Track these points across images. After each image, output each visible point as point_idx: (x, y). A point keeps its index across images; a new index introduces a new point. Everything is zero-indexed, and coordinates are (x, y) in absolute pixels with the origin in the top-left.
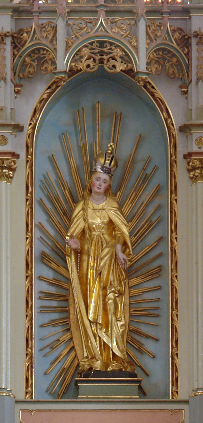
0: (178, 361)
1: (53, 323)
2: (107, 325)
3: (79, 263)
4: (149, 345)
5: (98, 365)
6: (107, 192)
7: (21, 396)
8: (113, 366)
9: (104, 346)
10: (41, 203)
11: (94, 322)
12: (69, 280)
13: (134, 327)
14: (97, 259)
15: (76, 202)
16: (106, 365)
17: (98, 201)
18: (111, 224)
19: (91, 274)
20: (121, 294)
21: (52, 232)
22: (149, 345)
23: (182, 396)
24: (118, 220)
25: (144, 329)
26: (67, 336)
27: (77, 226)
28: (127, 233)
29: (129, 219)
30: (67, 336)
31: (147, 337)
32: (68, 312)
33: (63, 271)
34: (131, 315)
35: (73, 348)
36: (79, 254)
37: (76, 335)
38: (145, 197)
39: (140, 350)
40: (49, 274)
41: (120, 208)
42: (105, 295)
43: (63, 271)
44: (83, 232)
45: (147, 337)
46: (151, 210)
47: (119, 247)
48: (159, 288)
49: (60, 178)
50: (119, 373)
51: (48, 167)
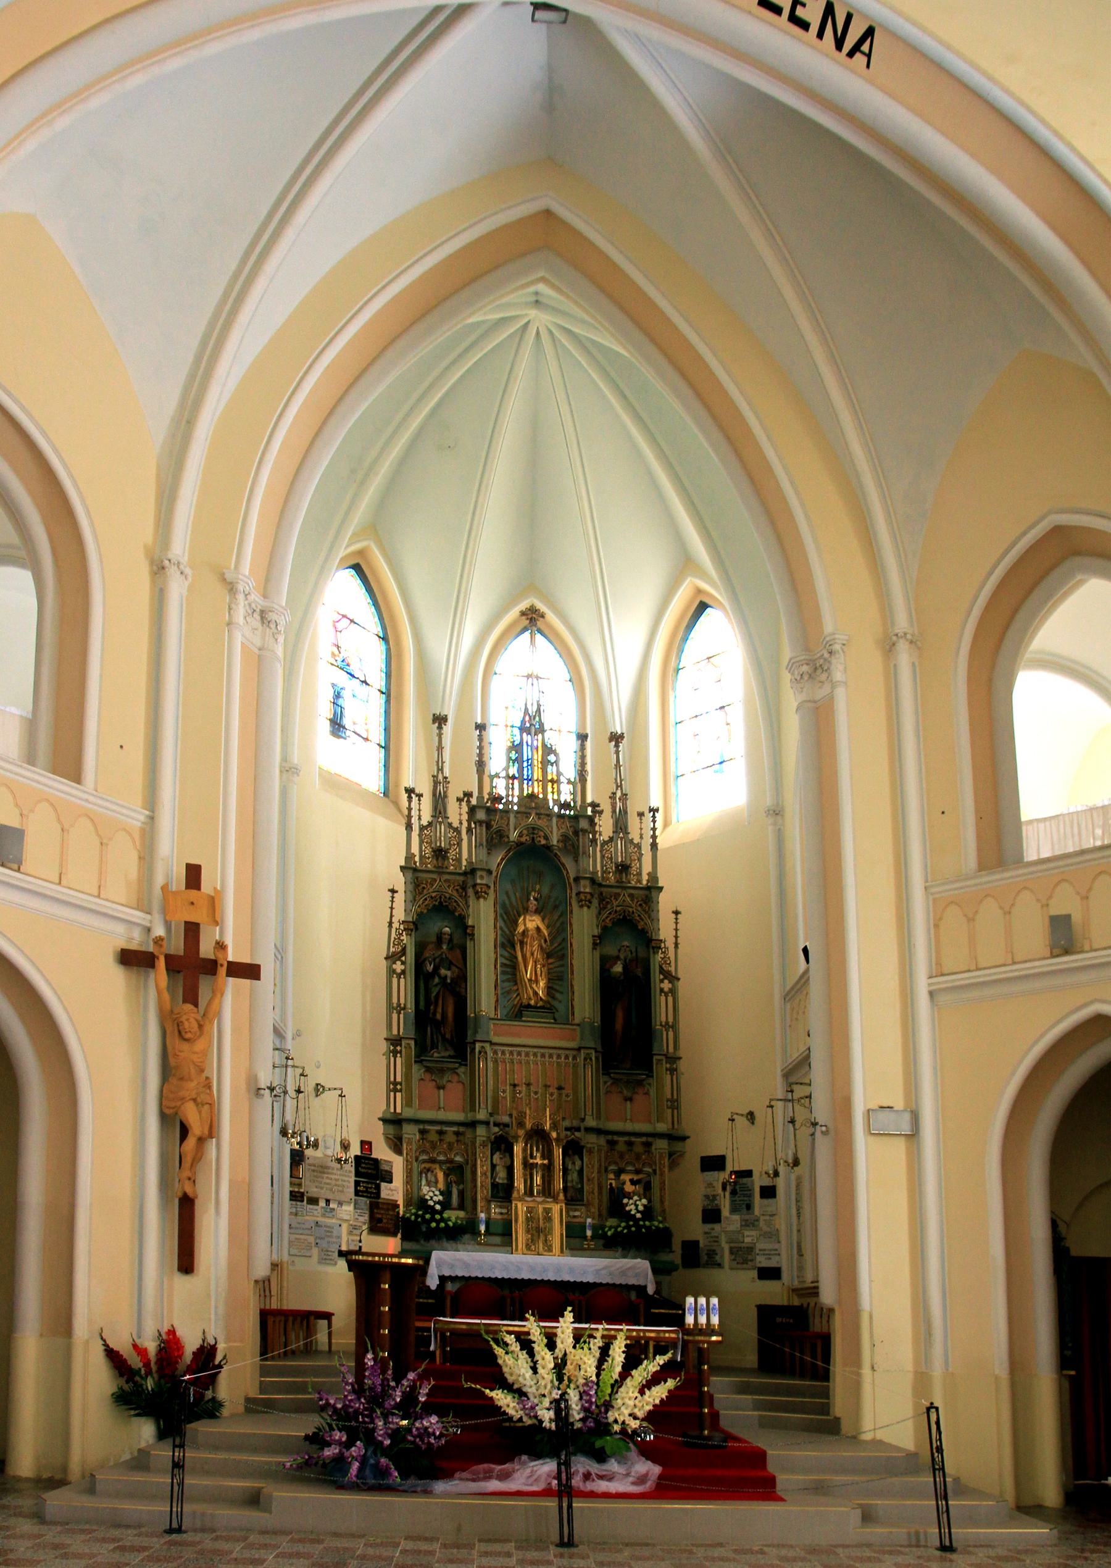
0: (574, 1003)
1: (508, 980)
2: (537, 982)
3: (522, 949)
4: (558, 995)
5: (532, 1002)
6: (537, 911)
7: (492, 1015)
8: (540, 1004)
9: (536, 994)
10: (501, 916)
11: (530, 980)
12: (516, 958)
13: (550, 985)
14: (532, 946)
15: (520, 916)
16: (536, 1003)
17: (531, 916)
18: (538, 929)
19: (528, 954)
20: (544, 966)
21: (508, 932)
22: (558, 995)
23: (577, 1021)
24: (542, 927)
25: (555, 987)
26: (515, 988)
27: (521, 929)
28: (546, 934)
29: (548, 927)
30: (515, 988)
31: (557, 991)
32: (516, 975)
33: (512, 952)
34: (549, 979)
35: (518, 994)
36: (522, 943)
37: (520, 987)
38: (556, 917)
39: (553, 997)
40: (506, 954)
41: (543, 920)
42: (536, 966)
43: (512, 952)
44: (524, 931)
45: (557, 991)
46: (558, 924)
47: (543, 941)
48: (562, 966)
49: (511, 904)
50: (542, 1007)
51: (505, 898)
